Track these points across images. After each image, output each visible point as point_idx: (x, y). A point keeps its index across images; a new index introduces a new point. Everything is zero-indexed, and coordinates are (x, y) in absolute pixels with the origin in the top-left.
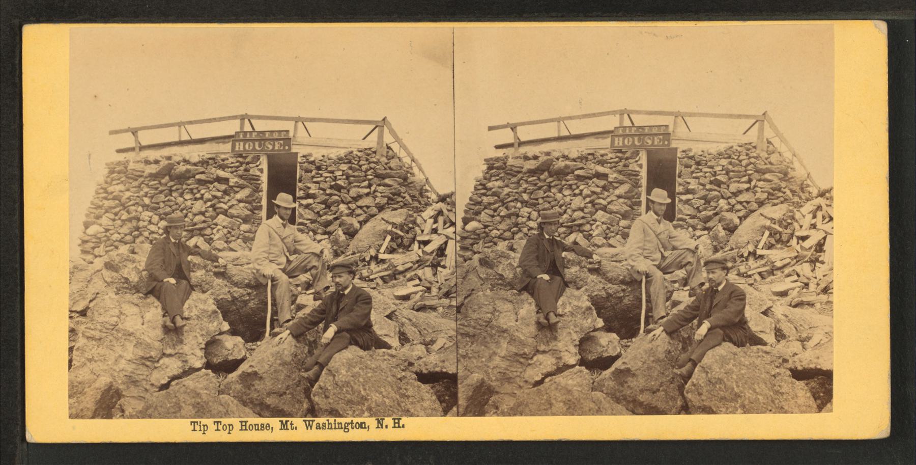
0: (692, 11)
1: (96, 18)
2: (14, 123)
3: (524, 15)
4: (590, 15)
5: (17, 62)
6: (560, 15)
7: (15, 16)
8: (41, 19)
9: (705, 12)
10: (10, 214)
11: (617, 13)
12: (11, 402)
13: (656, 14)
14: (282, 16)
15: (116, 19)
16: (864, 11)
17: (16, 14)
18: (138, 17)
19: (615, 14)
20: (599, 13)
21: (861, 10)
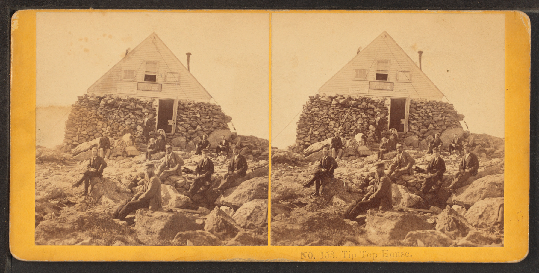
0: (417, 6)
1: (56, 6)
2: (6, 69)
3: (316, 7)
4: (356, 8)
5: (8, 32)
6: (337, 7)
7: (8, 4)
8: (23, 7)
9: (425, 7)
10: (3, 124)
11: (372, 7)
12: (2, 238)
13: (395, 8)
14: (169, 6)
15: (68, 6)
16: (522, 7)
17: (8, 3)
18: (82, 6)
19: (370, 7)
20: (361, 7)
21: (519, 7)
